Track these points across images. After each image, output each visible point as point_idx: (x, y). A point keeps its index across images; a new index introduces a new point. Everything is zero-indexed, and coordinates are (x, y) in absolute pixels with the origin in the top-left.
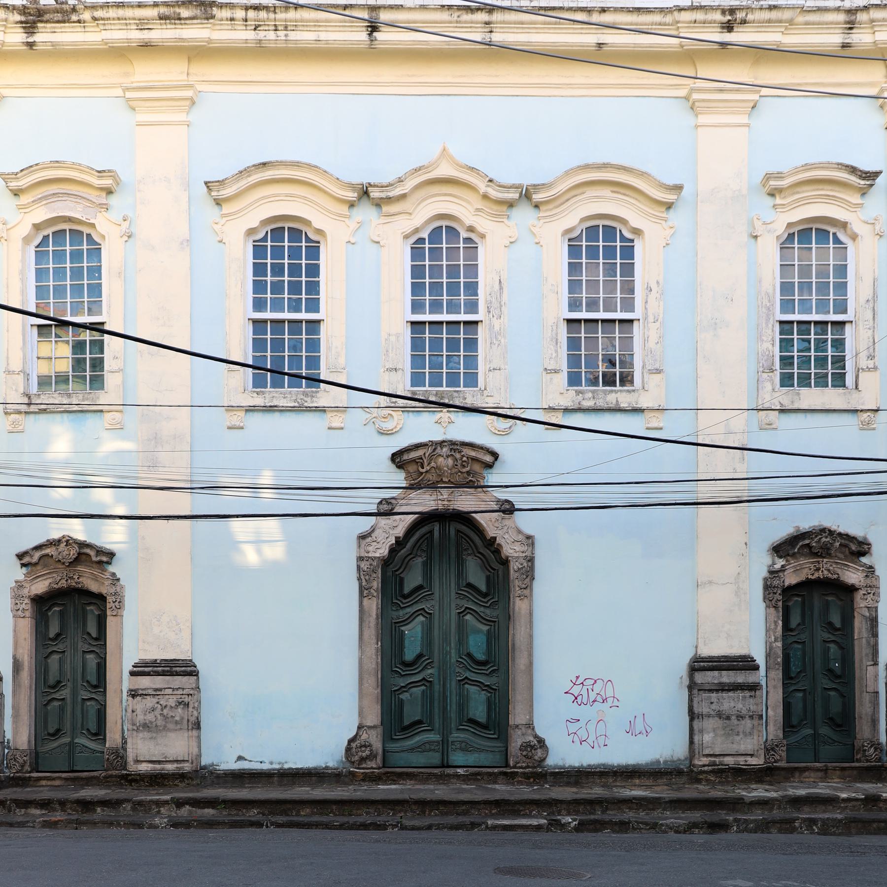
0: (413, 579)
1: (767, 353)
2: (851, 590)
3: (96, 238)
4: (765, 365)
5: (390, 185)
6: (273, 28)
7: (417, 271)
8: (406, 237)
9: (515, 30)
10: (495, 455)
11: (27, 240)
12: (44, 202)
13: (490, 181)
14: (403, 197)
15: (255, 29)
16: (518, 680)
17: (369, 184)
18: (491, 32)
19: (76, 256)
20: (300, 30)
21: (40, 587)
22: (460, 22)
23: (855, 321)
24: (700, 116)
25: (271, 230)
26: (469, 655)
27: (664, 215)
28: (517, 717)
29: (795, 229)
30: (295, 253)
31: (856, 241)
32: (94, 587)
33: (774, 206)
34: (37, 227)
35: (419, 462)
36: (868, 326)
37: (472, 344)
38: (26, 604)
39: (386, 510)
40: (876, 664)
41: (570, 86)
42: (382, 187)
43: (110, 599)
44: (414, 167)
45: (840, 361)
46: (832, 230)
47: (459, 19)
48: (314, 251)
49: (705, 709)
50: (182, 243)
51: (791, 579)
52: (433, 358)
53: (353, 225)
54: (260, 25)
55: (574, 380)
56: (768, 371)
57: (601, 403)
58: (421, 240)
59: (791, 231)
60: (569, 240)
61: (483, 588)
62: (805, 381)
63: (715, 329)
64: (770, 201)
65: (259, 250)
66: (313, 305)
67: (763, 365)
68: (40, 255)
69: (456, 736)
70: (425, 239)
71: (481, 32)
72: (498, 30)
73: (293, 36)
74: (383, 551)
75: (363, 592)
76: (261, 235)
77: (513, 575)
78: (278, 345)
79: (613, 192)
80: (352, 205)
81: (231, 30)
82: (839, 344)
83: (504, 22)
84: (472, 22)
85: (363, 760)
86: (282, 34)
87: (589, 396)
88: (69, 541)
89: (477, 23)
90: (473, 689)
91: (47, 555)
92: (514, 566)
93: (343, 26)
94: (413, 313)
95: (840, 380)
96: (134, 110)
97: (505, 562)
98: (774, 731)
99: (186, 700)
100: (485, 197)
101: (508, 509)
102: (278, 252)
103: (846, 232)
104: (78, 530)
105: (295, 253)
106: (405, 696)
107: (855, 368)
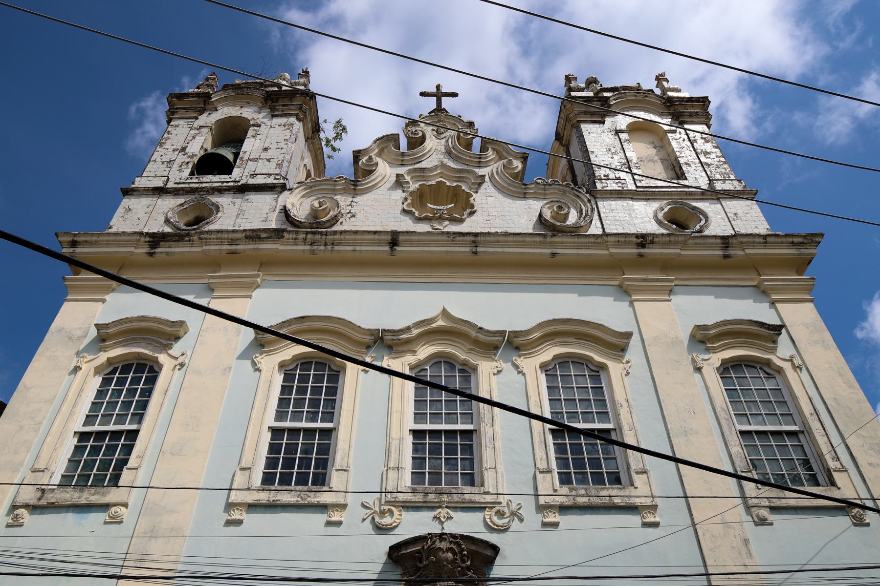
1: (739, 455)
3: (156, 368)
4: (741, 465)
5: (400, 330)
6: (324, 244)
12: (124, 344)
13: (481, 328)
14: (408, 341)
15: (311, 245)
17: (384, 330)
20: (343, 245)
23: (807, 431)
24: (632, 295)
25: (301, 364)
27: (621, 354)
29: (729, 365)
31: (781, 373)
33: (706, 349)
36: (821, 434)
37: (468, 449)
41: (535, 278)
42: (394, 332)
44: (420, 320)
50: (225, 370)
52: (433, 461)
54: (315, 243)
55: (565, 479)
56: (746, 470)
57: (595, 500)
59: (726, 366)
60: (546, 371)
63: (686, 435)
64: (703, 347)
67: (739, 465)
70: (427, 370)
73: (337, 248)
78: (291, 449)
79: (576, 339)
80: (368, 347)
81: (294, 245)
86: (329, 248)
87: (582, 495)
89: (466, 241)
94: (415, 423)
96: (214, 290)
100: (476, 342)
103: (769, 367)
105: (318, 379)
107: (824, 469)
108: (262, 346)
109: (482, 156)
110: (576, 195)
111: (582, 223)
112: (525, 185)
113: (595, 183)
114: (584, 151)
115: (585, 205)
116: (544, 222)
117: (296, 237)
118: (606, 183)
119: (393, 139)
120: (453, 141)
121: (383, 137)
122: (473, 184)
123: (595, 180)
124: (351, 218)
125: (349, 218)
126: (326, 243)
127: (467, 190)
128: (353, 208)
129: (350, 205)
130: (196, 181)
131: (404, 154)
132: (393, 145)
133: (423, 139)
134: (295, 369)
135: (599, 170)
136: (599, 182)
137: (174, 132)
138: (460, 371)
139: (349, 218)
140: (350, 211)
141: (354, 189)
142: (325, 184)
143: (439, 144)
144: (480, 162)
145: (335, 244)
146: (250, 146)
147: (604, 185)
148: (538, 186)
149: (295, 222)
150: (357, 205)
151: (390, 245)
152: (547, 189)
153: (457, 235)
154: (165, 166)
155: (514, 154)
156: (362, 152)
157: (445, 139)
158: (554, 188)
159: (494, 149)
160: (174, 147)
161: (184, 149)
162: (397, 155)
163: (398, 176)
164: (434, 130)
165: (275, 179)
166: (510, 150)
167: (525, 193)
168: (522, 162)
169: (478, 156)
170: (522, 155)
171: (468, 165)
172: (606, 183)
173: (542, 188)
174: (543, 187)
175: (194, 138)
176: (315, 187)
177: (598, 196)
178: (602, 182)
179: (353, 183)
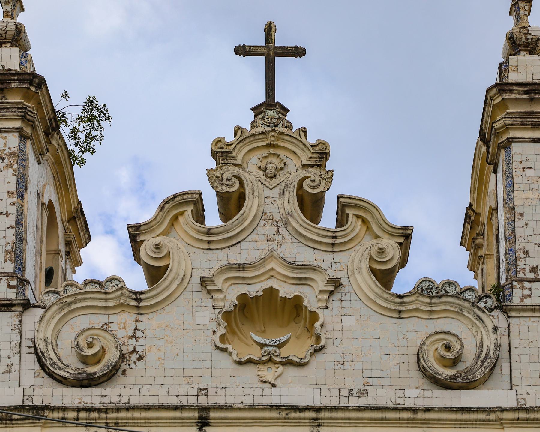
9: (343, 425)
18: (319, 426)
20: (131, 426)
22: (288, 418)
47: (287, 416)
71: (309, 426)
72: (325, 424)
83: (331, 418)
84: (300, 419)
89: (305, 419)
93: (173, 422)
109: (337, 234)
110: (478, 316)
111: (478, 373)
112: (401, 297)
113: (512, 287)
114: (510, 207)
115: (488, 335)
116: (423, 370)
117: (63, 416)
118: (530, 289)
120: (291, 199)
121: (175, 196)
122: (321, 292)
123: (514, 283)
124: (138, 363)
125: (135, 363)
126: (107, 423)
128: (138, 343)
129: (132, 337)
131: (212, 231)
132: (192, 211)
133: (241, 198)
135: (525, 256)
136: (518, 286)
139: (135, 363)
140: (135, 348)
141: (138, 307)
142: (90, 298)
143: (268, 201)
144: (333, 245)
145: (120, 425)
147: (527, 292)
148: (421, 298)
149: (54, 375)
150: (144, 335)
151: (198, 425)
152: (435, 303)
153: (292, 410)
155: (390, 229)
156: (142, 228)
157: (278, 188)
158: (445, 302)
159: (358, 217)
163: (204, 281)
164: (260, 167)
166: (382, 222)
167: (400, 311)
168: (400, 244)
169: (330, 234)
170: (401, 231)
171: (314, 249)
172: (530, 289)
173: (428, 303)
174: (428, 300)
176: (76, 303)
177: (513, 314)
178: (522, 288)
179: (134, 297)
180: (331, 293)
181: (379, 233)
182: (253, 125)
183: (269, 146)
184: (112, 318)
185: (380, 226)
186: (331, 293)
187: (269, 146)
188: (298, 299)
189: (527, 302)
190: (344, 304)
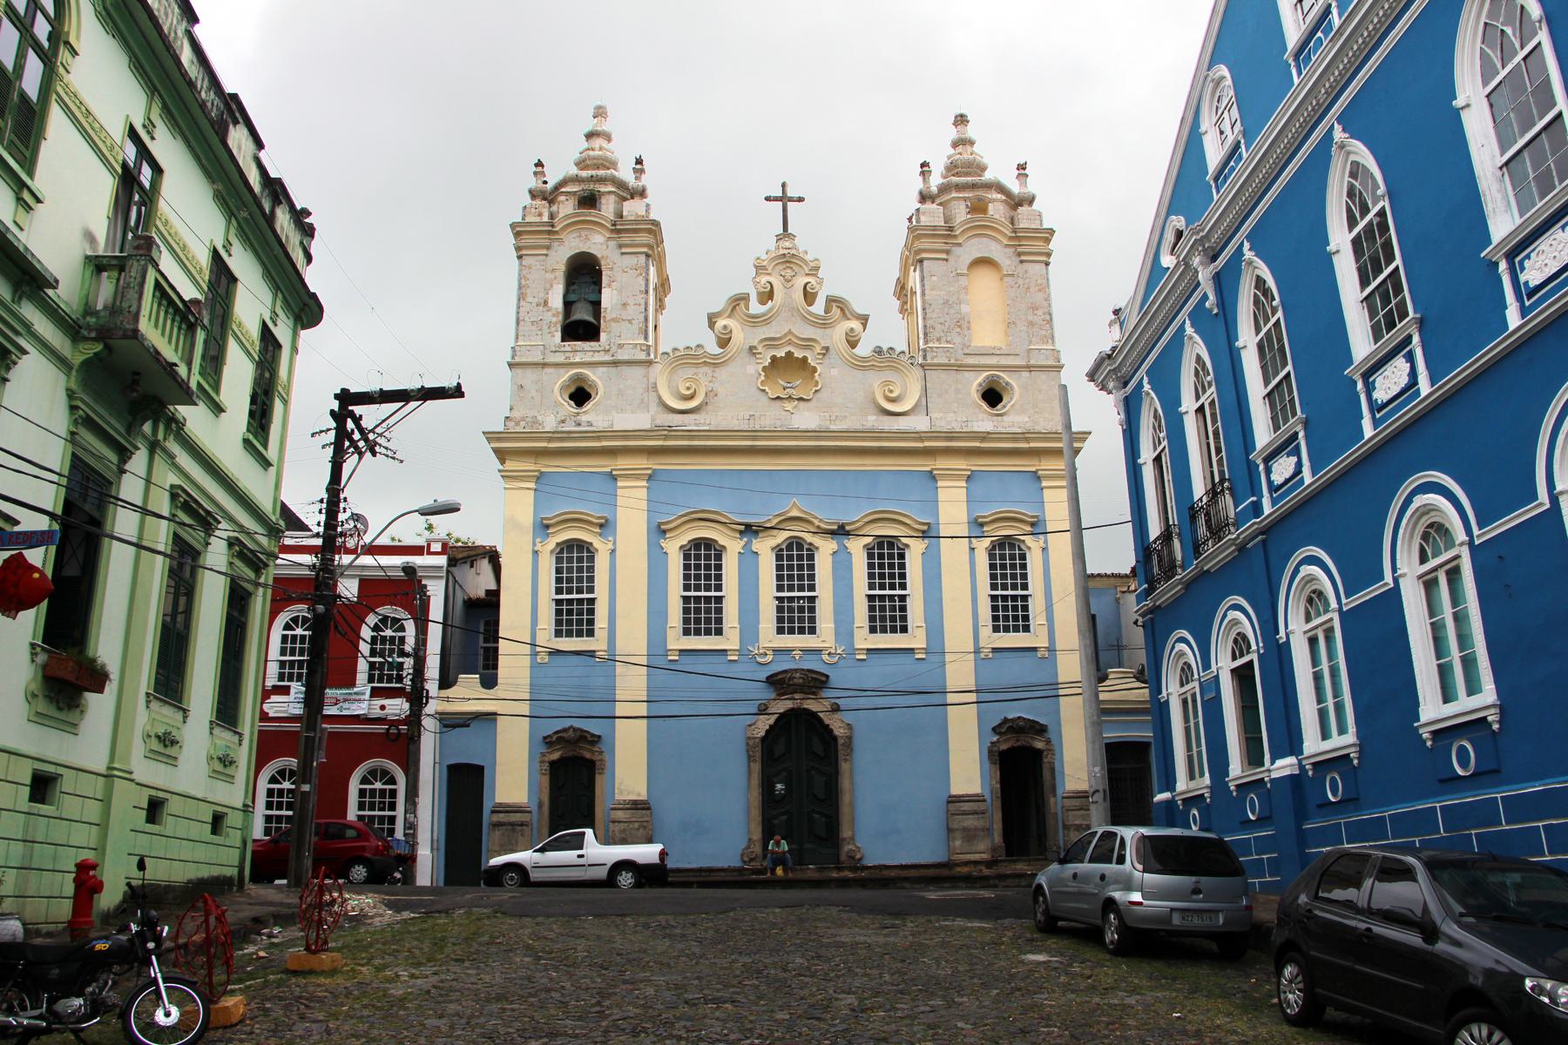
0: (779, 749)
2: (1039, 752)
3: (592, 549)
7: (779, 568)
8: (773, 549)
10: (827, 676)
11: (552, 552)
16: (845, 810)
19: (580, 560)
21: (556, 756)
26: (815, 796)
28: (845, 833)
30: (708, 557)
32: (588, 755)
34: (558, 544)
35: (782, 681)
38: (546, 766)
39: (763, 710)
40: (1055, 796)
43: (597, 763)
45: (1026, 618)
46: (1017, 543)
48: (719, 557)
49: (955, 826)
51: (1004, 747)
53: (742, 543)
58: (782, 550)
61: (822, 754)
62: (1006, 629)
65: (687, 557)
66: (719, 588)
68: (559, 560)
69: (807, 846)
74: (762, 734)
75: (750, 758)
76: (688, 548)
77: (840, 747)
82: (1025, 608)
85: (752, 860)
88: (575, 730)
90: (817, 816)
91: (560, 737)
92: (841, 741)
95: (1027, 629)
97: (835, 738)
98: (998, 838)
99: (645, 824)
101: (836, 709)
102: (698, 557)
104: (577, 723)
105: (708, 557)
106: (776, 822)
108: (664, 532)
119: (742, 299)
122: (819, 354)
127: (812, 364)
130: (570, 349)
134: (690, 549)
137: (529, 276)
138: (808, 550)
146: (608, 298)
154: (534, 328)
160: (536, 300)
161: (546, 303)
162: (749, 317)
165: (642, 350)
175: (552, 286)
180: (824, 354)
181: (850, 316)
182: (778, 248)
183: (787, 262)
184: (699, 370)
185: (851, 313)
186: (824, 354)
187: (787, 262)
188: (805, 359)
189: (935, 361)
190: (832, 361)
